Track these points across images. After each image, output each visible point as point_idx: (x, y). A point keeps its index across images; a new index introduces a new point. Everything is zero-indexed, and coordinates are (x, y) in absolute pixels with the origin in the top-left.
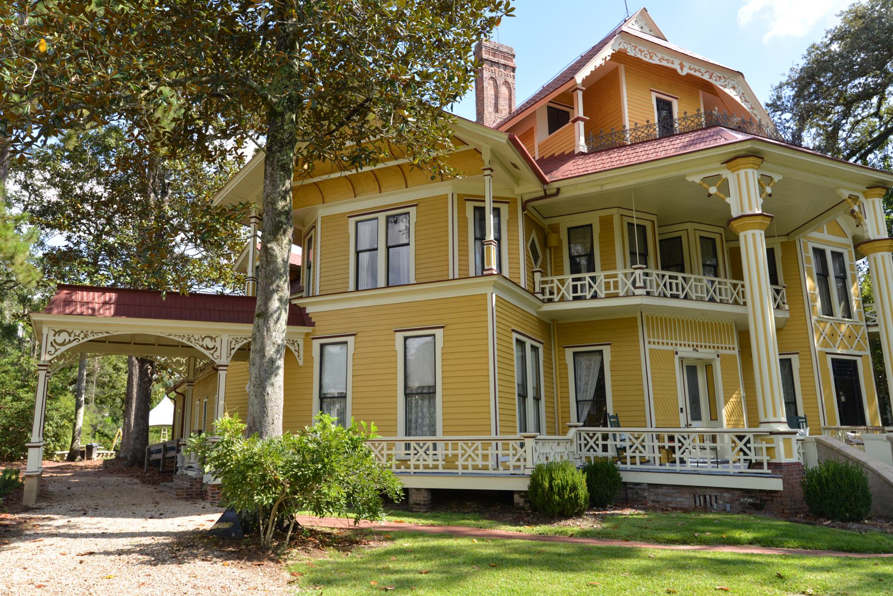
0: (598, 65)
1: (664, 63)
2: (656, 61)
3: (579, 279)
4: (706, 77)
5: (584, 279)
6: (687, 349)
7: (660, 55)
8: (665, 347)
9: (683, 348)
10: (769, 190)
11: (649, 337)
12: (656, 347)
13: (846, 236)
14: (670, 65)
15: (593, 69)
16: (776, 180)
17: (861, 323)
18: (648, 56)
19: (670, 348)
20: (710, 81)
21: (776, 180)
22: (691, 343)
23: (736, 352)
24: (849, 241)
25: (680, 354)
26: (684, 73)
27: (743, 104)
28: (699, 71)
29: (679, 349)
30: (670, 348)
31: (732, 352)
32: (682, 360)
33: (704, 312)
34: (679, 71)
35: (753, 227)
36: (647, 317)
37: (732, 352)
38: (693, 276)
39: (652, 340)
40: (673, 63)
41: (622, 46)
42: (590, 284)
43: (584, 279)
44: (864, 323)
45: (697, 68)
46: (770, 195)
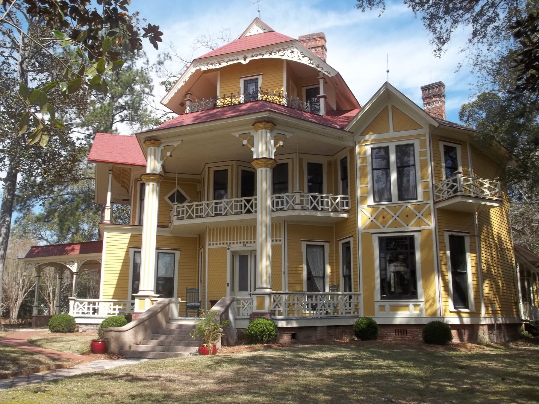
0: (179, 87)
1: (230, 63)
2: (224, 64)
3: (279, 198)
4: (267, 56)
5: (283, 197)
6: (239, 245)
7: (226, 60)
8: (222, 246)
9: (235, 245)
10: (168, 154)
11: (210, 241)
12: (215, 246)
13: (420, 127)
14: (236, 62)
15: (176, 91)
16: (175, 146)
17: (425, 202)
18: (218, 65)
19: (225, 246)
20: (271, 57)
21: (175, 146)
22: (242, 241)
23: (282, 243)
24: (426, 131)
25: (232, 249)
26: (248, 61)
27: (300, 61)
28: (260, 55)
29: (232, 245)
30: (225, 246)
31: (278, 243)
32: (233, 254)
33: (241, 221)
34: (243, 62)
35: (152, 181)
36: (210, 229)
37: (278, 243)
38: (233, 200)
39: (212, 243)
40: (238, 59)
41: (198, 68)
42: (245, 204)
43: (283, 197)
44: (431, 202)
45: (258, 53)
46: (171, 156)
